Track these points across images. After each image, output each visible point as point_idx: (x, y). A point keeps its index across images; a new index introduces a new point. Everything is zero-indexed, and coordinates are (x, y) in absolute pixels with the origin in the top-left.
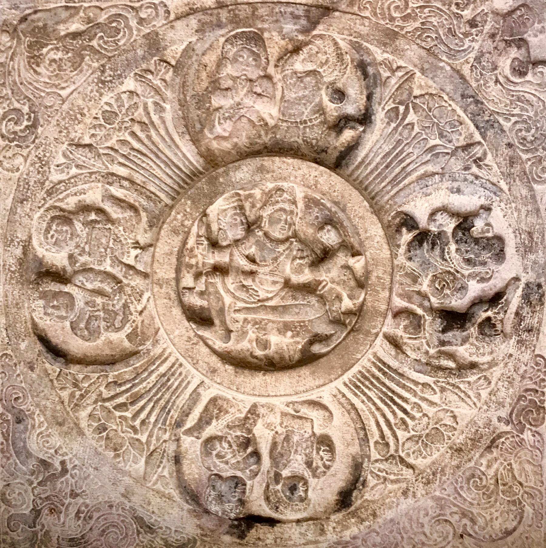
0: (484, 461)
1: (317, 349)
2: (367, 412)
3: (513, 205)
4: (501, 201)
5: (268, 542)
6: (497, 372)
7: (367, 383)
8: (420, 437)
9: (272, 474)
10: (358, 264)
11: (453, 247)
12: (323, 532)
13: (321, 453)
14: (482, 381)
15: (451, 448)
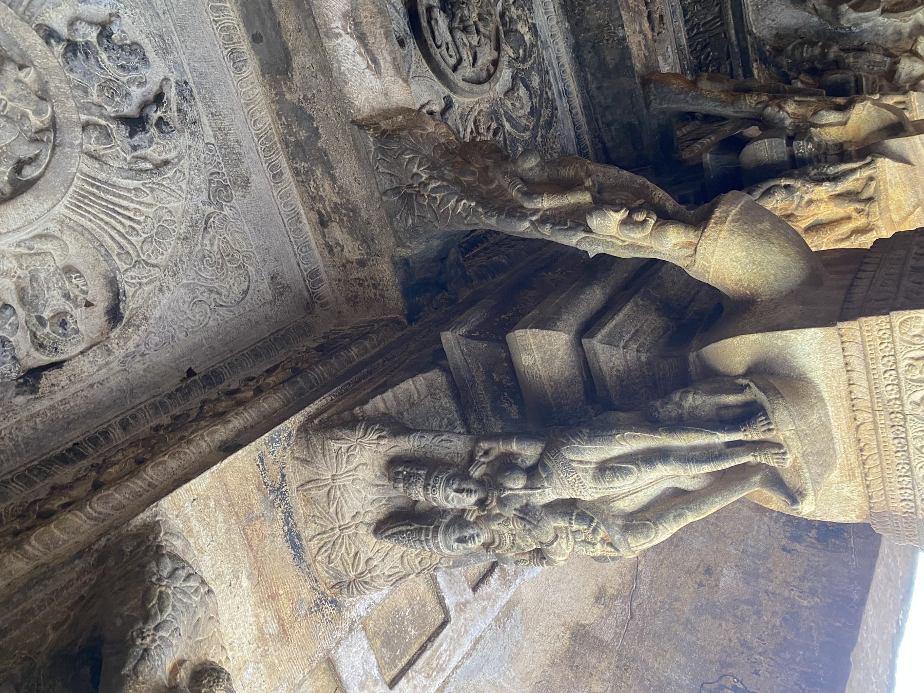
0: (207, 242)
1: (30, 172)
2: (98, 230)
3: (138, 11)
4: (126, 7)
5: (62, 384)
6: (185, 163)
7: (86, 201)
8: (152, 237)
9: (35, 321)
10: (29, 76)
11: (104, 56)
12: (109, 352)
13: (73, 280)
14: (178, 174)
15: (179, 239)
